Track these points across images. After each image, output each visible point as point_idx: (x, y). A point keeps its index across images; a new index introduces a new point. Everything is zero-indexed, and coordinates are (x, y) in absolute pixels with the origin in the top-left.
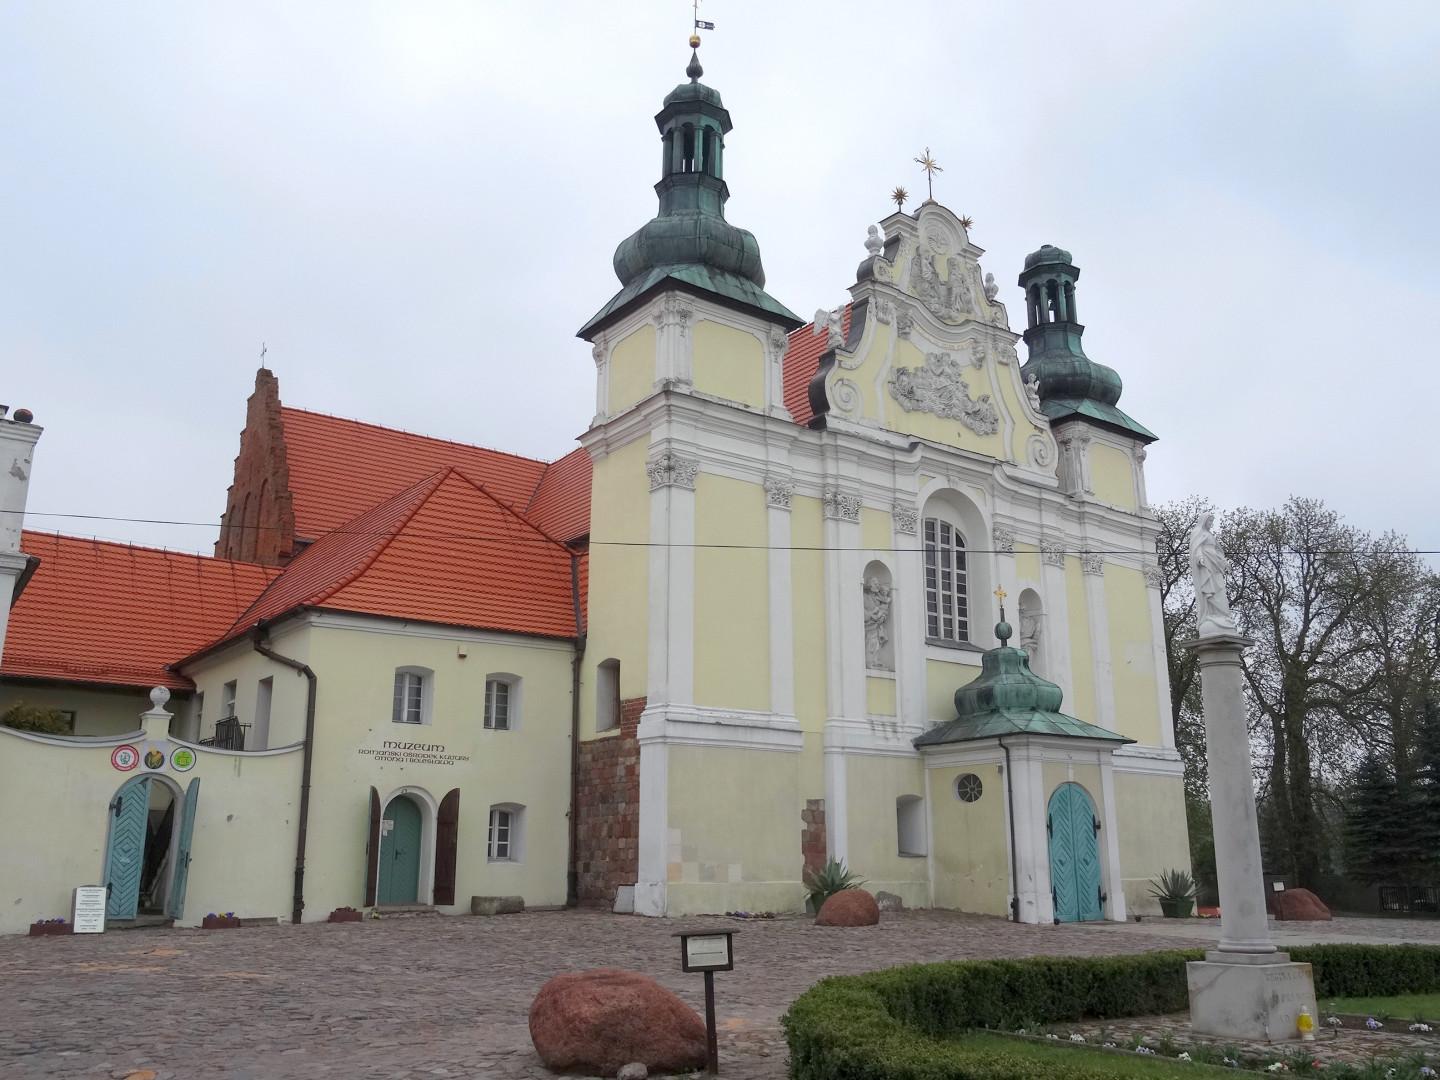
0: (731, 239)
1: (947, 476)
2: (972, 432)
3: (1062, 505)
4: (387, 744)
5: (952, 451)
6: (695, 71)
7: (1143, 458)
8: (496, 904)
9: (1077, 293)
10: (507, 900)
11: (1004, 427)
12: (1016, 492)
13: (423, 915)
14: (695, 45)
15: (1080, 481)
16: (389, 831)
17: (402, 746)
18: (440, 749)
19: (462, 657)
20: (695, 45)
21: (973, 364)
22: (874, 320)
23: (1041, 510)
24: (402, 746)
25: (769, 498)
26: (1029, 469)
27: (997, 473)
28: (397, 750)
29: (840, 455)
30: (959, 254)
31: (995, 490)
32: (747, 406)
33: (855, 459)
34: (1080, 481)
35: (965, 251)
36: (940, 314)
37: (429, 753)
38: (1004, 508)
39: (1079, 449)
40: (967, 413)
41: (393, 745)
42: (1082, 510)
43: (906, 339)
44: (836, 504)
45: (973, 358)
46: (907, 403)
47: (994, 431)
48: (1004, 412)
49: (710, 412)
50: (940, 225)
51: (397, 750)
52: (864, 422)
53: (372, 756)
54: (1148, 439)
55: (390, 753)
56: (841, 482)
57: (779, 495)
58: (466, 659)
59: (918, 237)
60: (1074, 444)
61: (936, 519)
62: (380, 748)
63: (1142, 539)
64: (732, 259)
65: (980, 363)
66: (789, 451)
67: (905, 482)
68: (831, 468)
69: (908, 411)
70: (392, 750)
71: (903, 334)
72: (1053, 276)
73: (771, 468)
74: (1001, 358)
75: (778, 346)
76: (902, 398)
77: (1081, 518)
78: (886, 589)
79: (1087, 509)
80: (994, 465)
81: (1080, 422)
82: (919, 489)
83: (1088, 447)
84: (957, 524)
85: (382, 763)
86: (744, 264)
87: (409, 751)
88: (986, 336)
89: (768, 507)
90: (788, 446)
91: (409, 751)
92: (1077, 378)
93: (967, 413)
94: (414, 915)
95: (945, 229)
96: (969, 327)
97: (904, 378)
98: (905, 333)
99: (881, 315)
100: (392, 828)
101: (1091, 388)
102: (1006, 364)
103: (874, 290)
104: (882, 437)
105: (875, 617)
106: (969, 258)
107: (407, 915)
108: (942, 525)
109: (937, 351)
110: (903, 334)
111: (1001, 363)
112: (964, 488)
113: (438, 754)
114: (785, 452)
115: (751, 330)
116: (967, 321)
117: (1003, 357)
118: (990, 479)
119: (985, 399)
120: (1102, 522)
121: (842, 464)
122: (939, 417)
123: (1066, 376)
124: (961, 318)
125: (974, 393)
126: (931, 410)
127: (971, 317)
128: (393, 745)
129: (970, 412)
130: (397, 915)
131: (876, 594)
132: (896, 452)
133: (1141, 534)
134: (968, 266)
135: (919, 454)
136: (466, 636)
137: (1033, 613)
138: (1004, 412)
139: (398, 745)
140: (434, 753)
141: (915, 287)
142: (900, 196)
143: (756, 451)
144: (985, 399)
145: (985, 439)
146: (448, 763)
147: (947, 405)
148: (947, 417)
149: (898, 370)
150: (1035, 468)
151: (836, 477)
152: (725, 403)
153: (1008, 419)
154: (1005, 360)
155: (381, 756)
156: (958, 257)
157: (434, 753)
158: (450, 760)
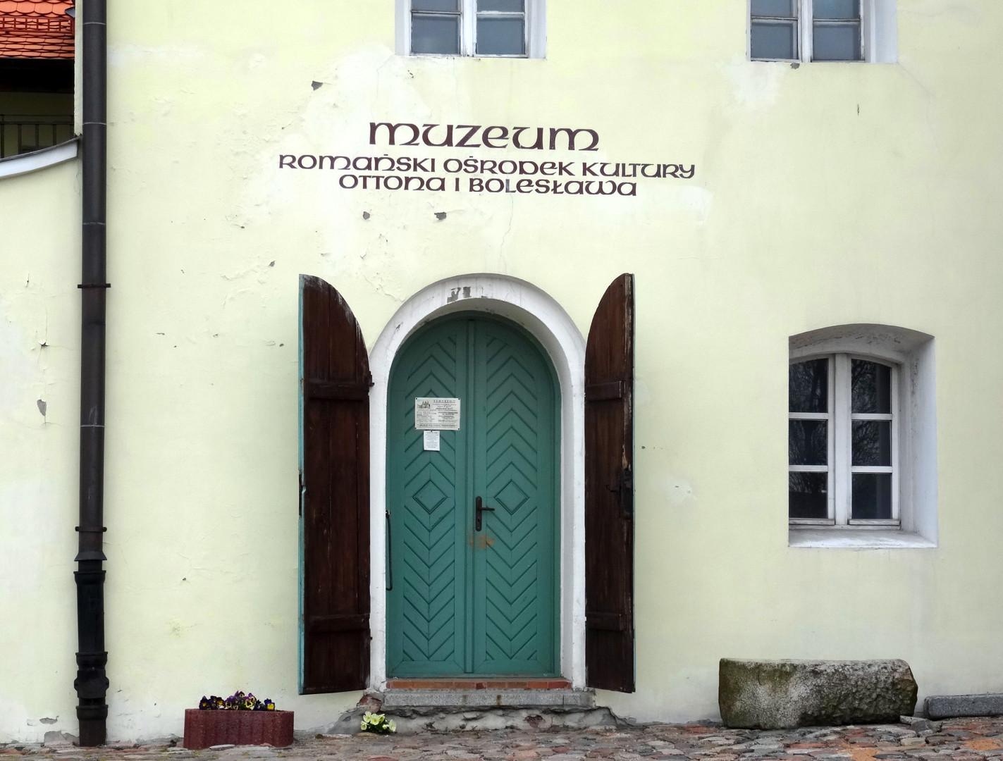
4: (383, 133)
8: (798, 691)
10: (840, 675)
13: (549, 721)
16: (445, 436)
17: (438, 135)
18: (583, 140)
24: (438, 135)
28: (420, 152)
37: (539, 156)
41: (404, 134)
51: (420, 152)
53: (329, 176)
62: (359, 147)
70: (397, 152)
85: (370, 197)
87: (463, 154)
91: (463, 154)
94: (519, 720)
100: (456, 424)
107: (494, 722)
113: (576, 159)
128: (404, 134)
130: (455, 722)
139: (421, 134)
140: (561, 154)
146: (617, 188)
157: (561, 154)
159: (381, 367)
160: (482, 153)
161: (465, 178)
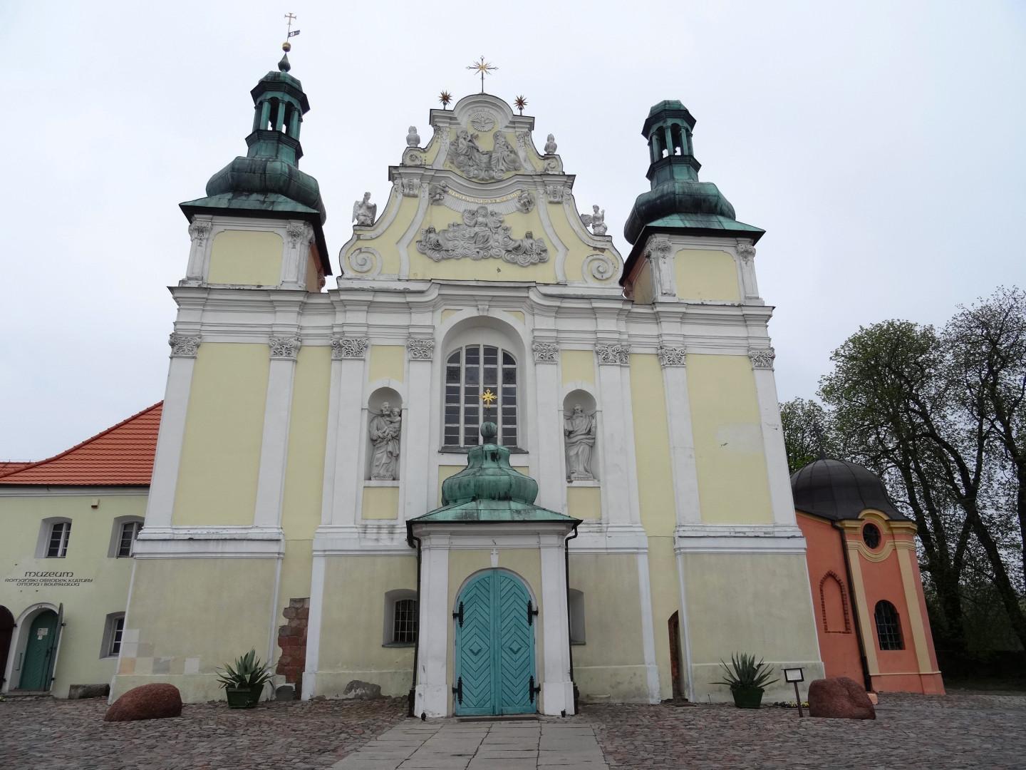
0: (253, 167)
1: (477, 306)
2: (516, 265)
3: (621, 310)
5: (512, 285)
6: (284, 66)
7: (752, 254)
9: (693, 139)
11: (555, 257)
12: (559, 307)
13: (40, 698)
14: (287, 49)
15: (659, 286)
16: (44, 636)
17: (39, 574)
18: (70, 575)
19: (95, 507)
20: (287, 49)
21: (519, 210)
22: (400, 196)
23: (596, 319)
24: (39, 574)
25: (272, 353)
26: (586, 286)
27: (533, 295)
29: (348, 308)
30: (507, 127)
31: (534, 309)
33: (366, 308)
34: (659, 286)
35: (511, 122)
36: (481, 177)
37: (60, 578)
38: (546, 323)
39: (658, 258)
40: (508, 251)
41: (33, 574)
42: (655, 310)
43: (439, 205)
44: (344, 348)
45: (518, 205)
46: (437, 255)
47: (543, 261)
48: (555, 241)
50: (486, 109)
51: (35, 578)
52: (382, 278)
53: (15, 583)
54: (755, 235)
55: (30, 580)
56: (345, 329)
57: (285, 349)
58: (99, 509)
59: (459, 124)
60: (653, 255)
61: (479, 345)
62: (22, 576)
63: (746, 326)
64: (256, 181)
65: (527, 205)
66: (299, 313)
67: (421, 319)
68: (340, 318)
69: (438, 261)
71: (435, 200)
72: (661, 124)
73: (274, 329)
74: (552, 199)
75: (295, 236)
76: (429, 252)
77: (657, 318)
78: (396, 410)
79: (659, 309)
80: (528, 288)
81: (656, 235)
82: (441, 323)
83: (670, 257)
84: (501, 344)
85: (23, 587)
86: (268, 183)
88: (535, 185)
89: (271, 360)
90: (297, 309)
92: (665, 199)
93: (508, 251)
94: (33, 698)
95: (492, 111)
97: (432, 235)
98: (437, 200)
99: (407, 191)
100: (46, 634)
101: (678, 203)
102: (558, 203)
103: (400, 174)
104: (401, 286)
105: (381, 436)
106: (518, 127)
107: (29, 699)
108: (485, 350)
109: (474, 207)
110: (435, 200)
111: (551, 203)
112: (498, 314)
114: (294, 315)
117: (555, 197)
118: (527, 300)
119: (529, 236)
120: (684, 318)
121: (348, 314)
122: (475, 259)
123: (656, 199)
125: (518, 235)
126: (465, 256)
128: (33, 574)
129: (510, 249)
130: (20, 699)
131: (389, 416)
132: (407, 295)
133: (745, 321)
134: (517, 134)
136: (99, 492)
137: (591, 412)
138: (555, 241)
139: (36, 574)
140: (65, 578)
141: (452, 163)
142: (445, 98)
143: (265, 319)
144: (529, 236)
145: (531, 268)
146: (75, 584)
147: (481, 249)
148: (485, 258)
149: (427, 231)
150: (596, 284)
151: (342, 325)
152: (237, 288)
153: (561, 248)
154: (556, 200)
155: (22, 582)
156: (506, 130)
157: (65, 578)
158: (77, 583)
159: (19, 623)
160: (48, 578)
161: (44, 583)
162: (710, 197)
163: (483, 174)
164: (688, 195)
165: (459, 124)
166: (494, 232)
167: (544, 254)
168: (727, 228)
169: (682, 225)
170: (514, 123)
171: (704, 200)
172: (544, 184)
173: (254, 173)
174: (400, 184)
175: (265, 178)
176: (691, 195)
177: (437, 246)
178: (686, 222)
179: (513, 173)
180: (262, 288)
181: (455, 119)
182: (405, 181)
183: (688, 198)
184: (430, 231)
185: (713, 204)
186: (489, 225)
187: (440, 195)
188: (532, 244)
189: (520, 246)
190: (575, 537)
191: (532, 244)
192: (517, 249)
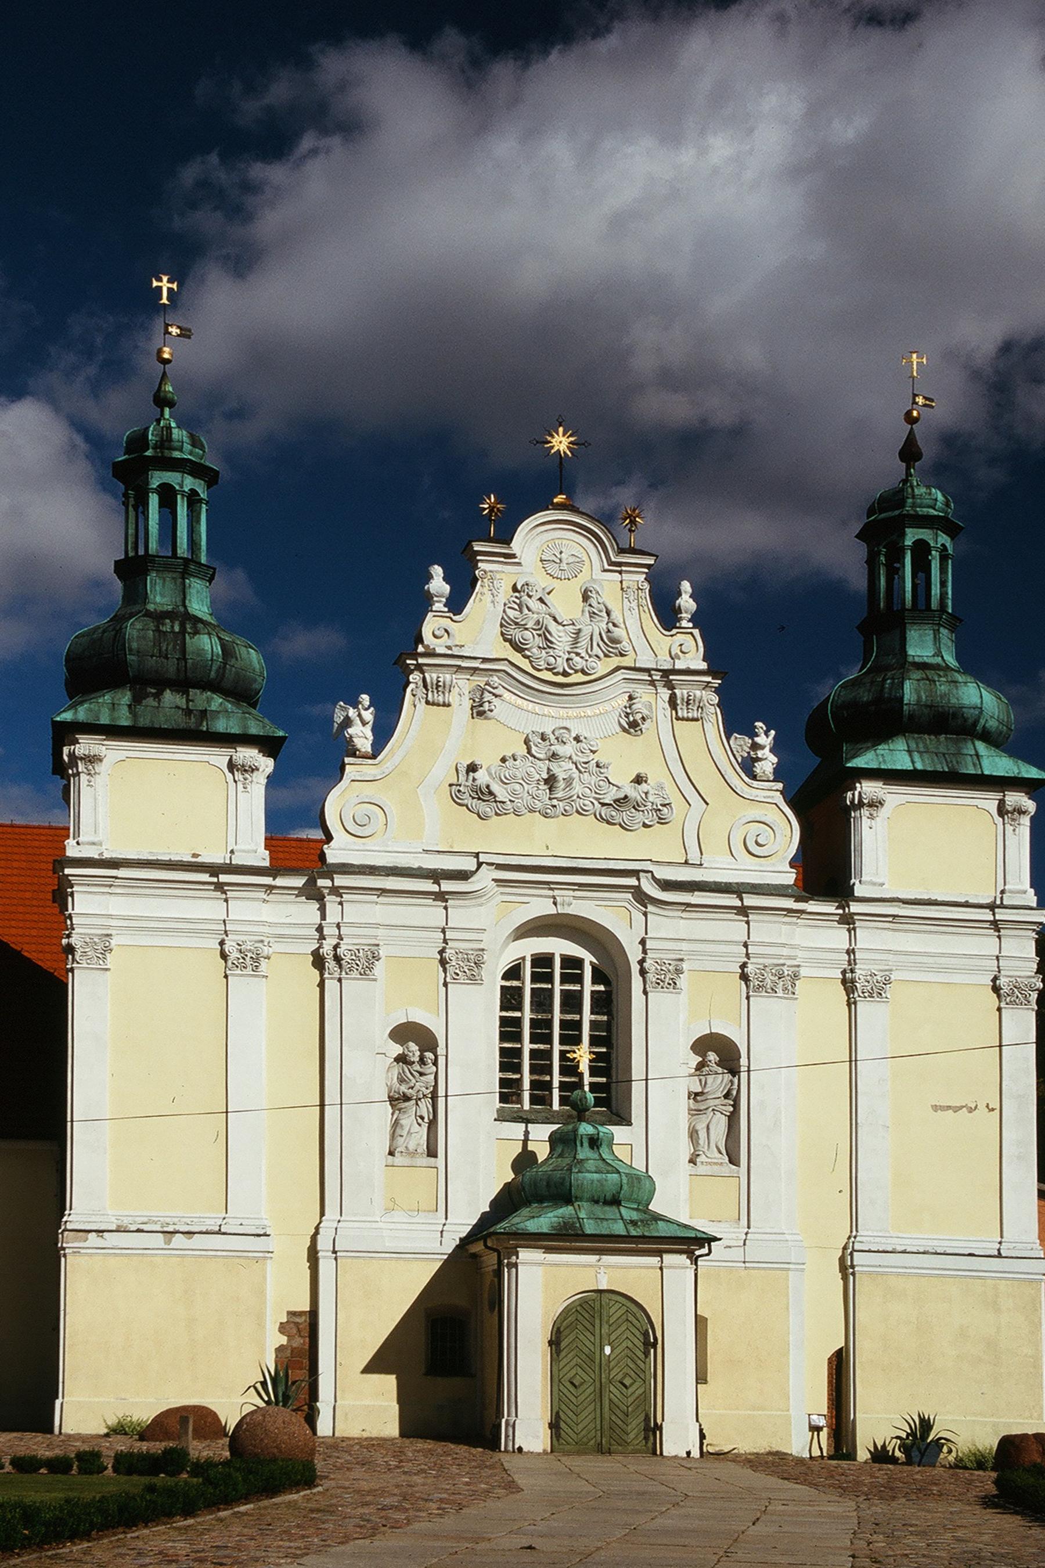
22: (422, 706)
32: (195, 855)
49: (122, 873)
96: (620, 675)
101: (905, 720)
115: (206, 758)
116: (618, 669)
124: (601, 667)
125: (621, 777)
127: (627, 662)
129: (607, 801)
135: (485, 878)
162: (964, 710)
163: (561, 665)
164: (926, 706)
165: (519, 564)
166: (583, 770)
167: (665, 810)
168: (986, 772)
169: (909, 766)
170: (620, 564)
171: (954, 715)
172: (670, 686)
173: (167, 658)
174: (421, 683)
175: (186, 666)
176: (931, 707)
177: (484, 794)
178: (916, 756)
179: (616, 661)
180: (199, 860)
181: (513, 556)
182: (431, 676)
183: (926, 711)
184: (472, 768)
185: (970, 721)
186: (575, 758)
187: (490, 702)
188: (646, 793)
189: (626, 797)
190: (708, 1255)
191: (646, 793)
192: (622, 802)
